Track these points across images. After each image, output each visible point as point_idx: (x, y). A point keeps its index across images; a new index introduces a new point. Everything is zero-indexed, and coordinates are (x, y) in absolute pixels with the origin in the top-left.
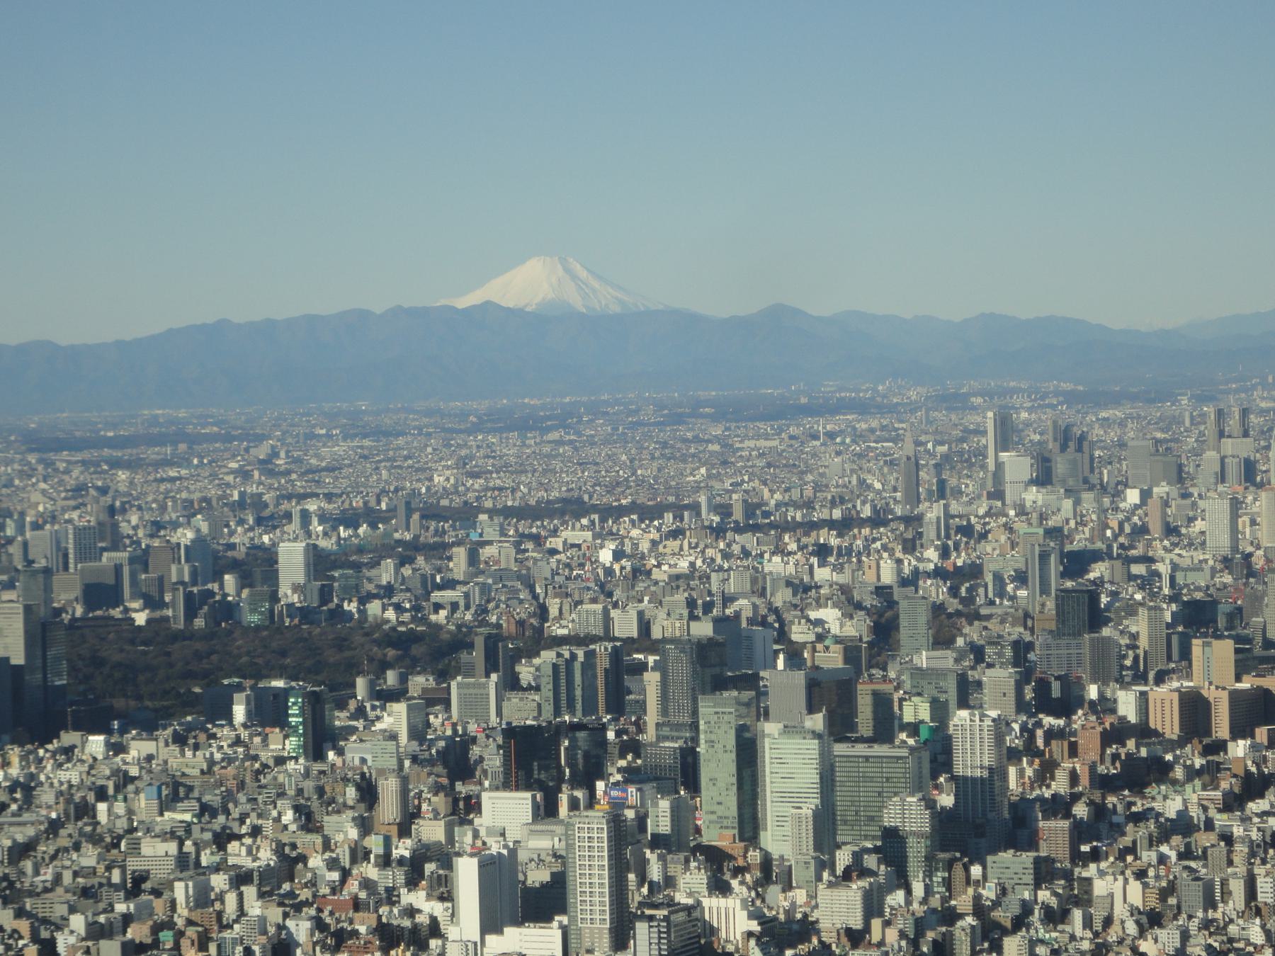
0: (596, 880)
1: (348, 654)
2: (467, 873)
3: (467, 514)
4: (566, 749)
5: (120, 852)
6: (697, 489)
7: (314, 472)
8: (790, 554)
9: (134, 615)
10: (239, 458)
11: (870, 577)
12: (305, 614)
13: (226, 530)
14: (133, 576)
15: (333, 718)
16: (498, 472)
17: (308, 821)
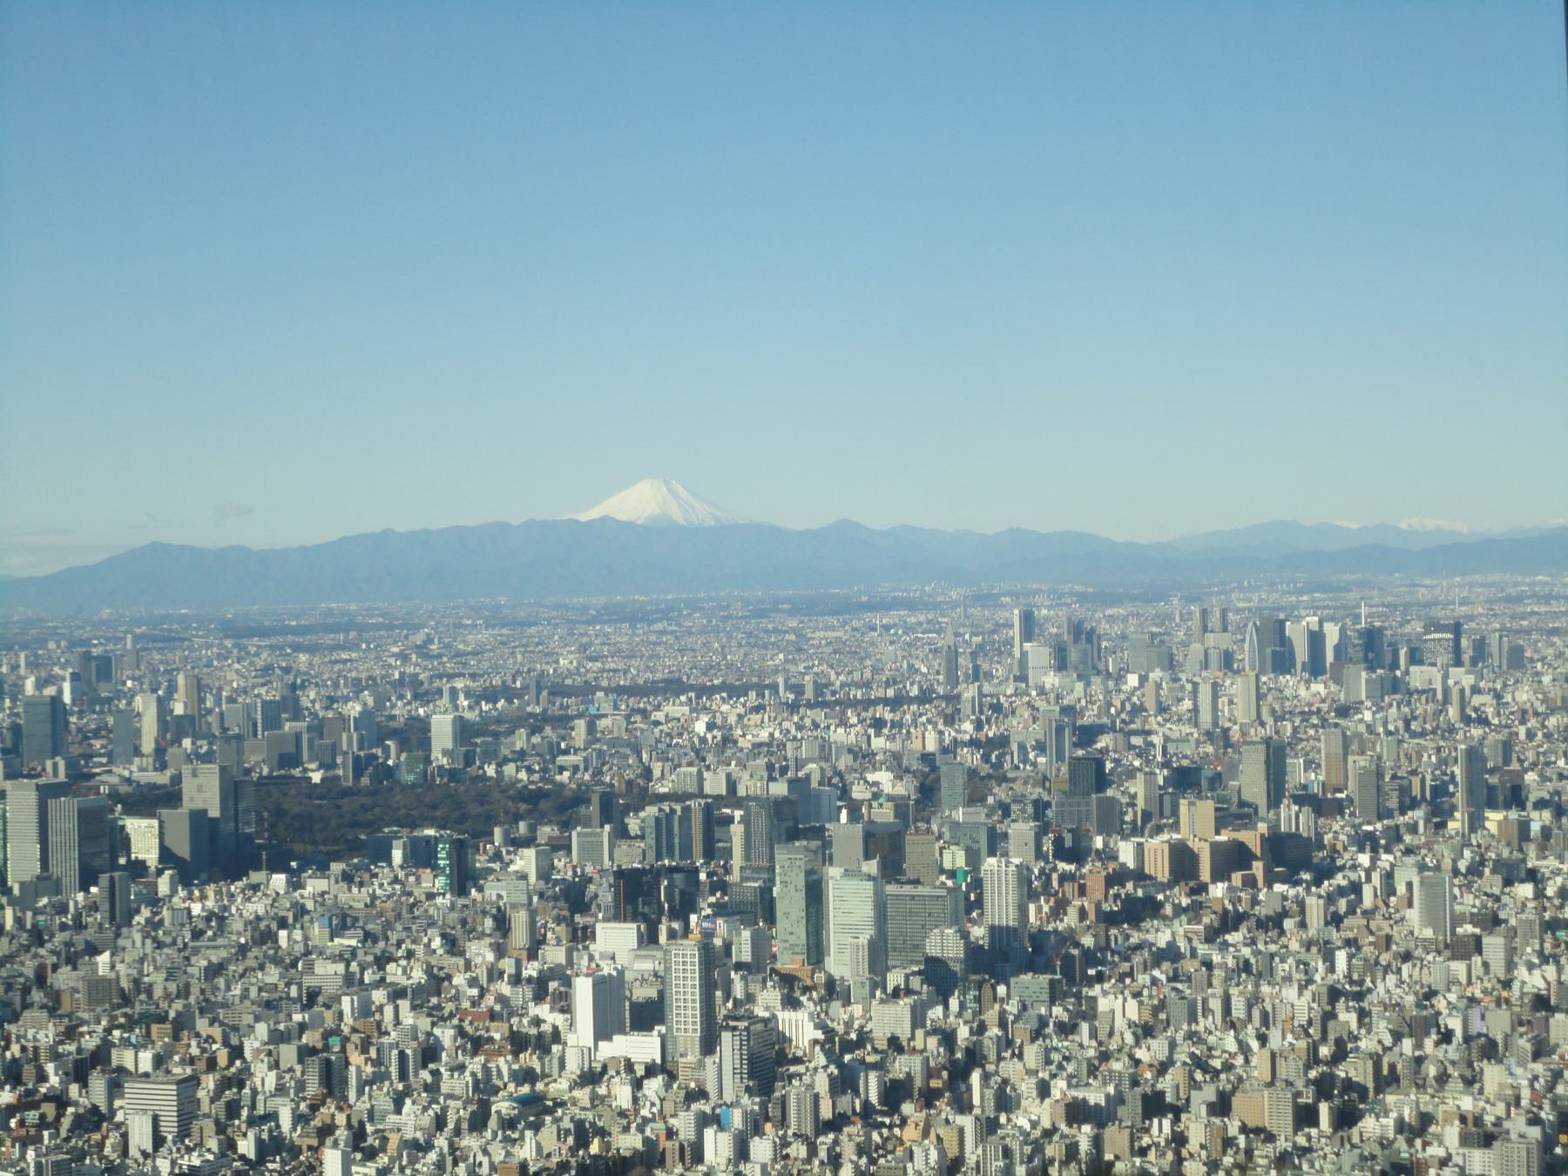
0: (689, 997)
1: (487, 807)
2: (583, 991)
3: (586, 691)
6: (776, 671)
7: (461, 656)
8: (851, 726)
9: (311, 774)
11: (916, 745)
12: (452, 774)
14: (310, 741)
15: (475, 861)
17: (453, 946)
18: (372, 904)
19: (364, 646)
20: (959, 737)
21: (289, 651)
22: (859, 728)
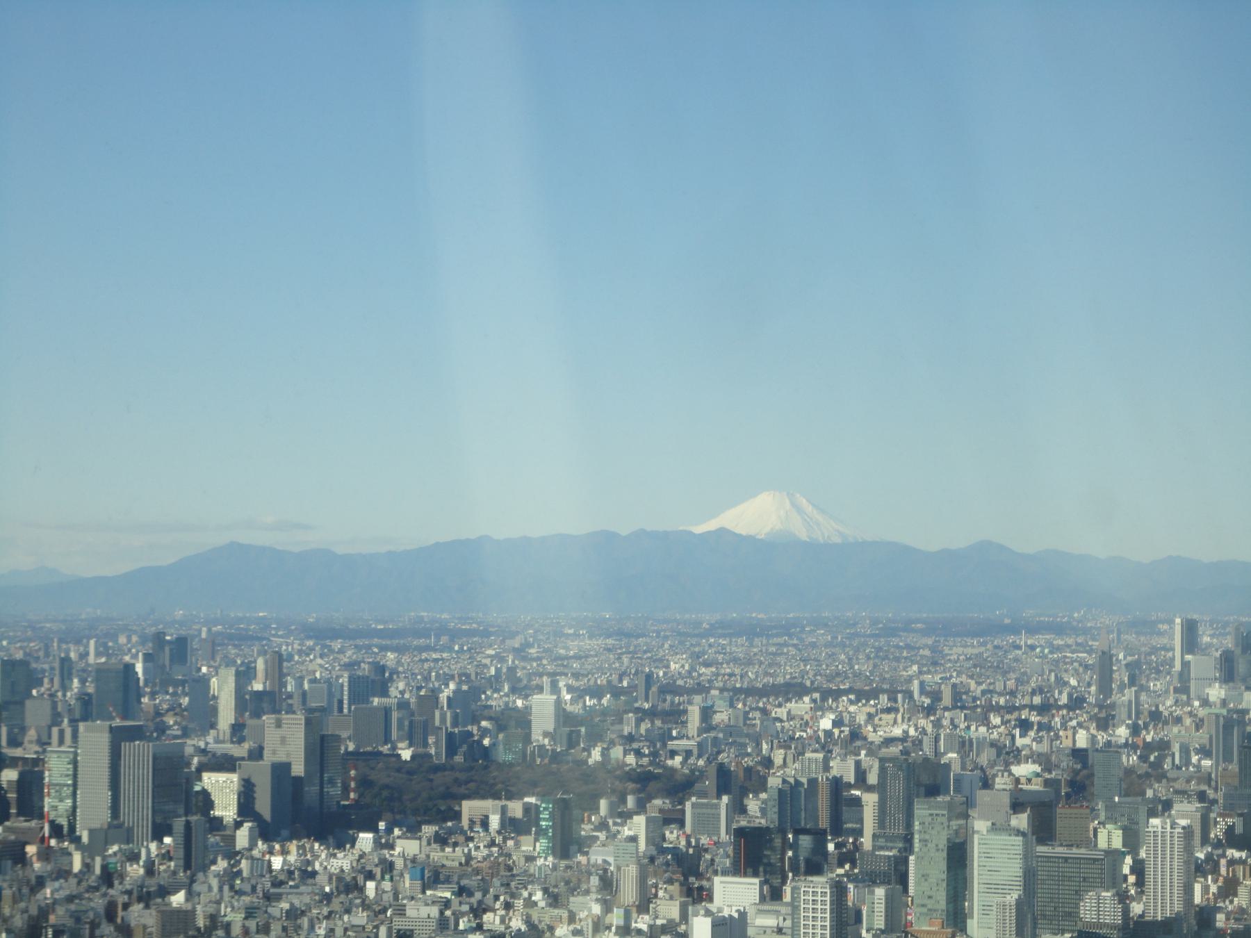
3: (701, 689)
6: (909, 680)
8: (995, 727)
9: (400, 752)
11: (1067, 743)
12: (555, 757)
16: (728, 663)
18: (467, 863)
19: (456, 648)
20: (1114, 739)
21: (376, 650)
22: (1002, 729)
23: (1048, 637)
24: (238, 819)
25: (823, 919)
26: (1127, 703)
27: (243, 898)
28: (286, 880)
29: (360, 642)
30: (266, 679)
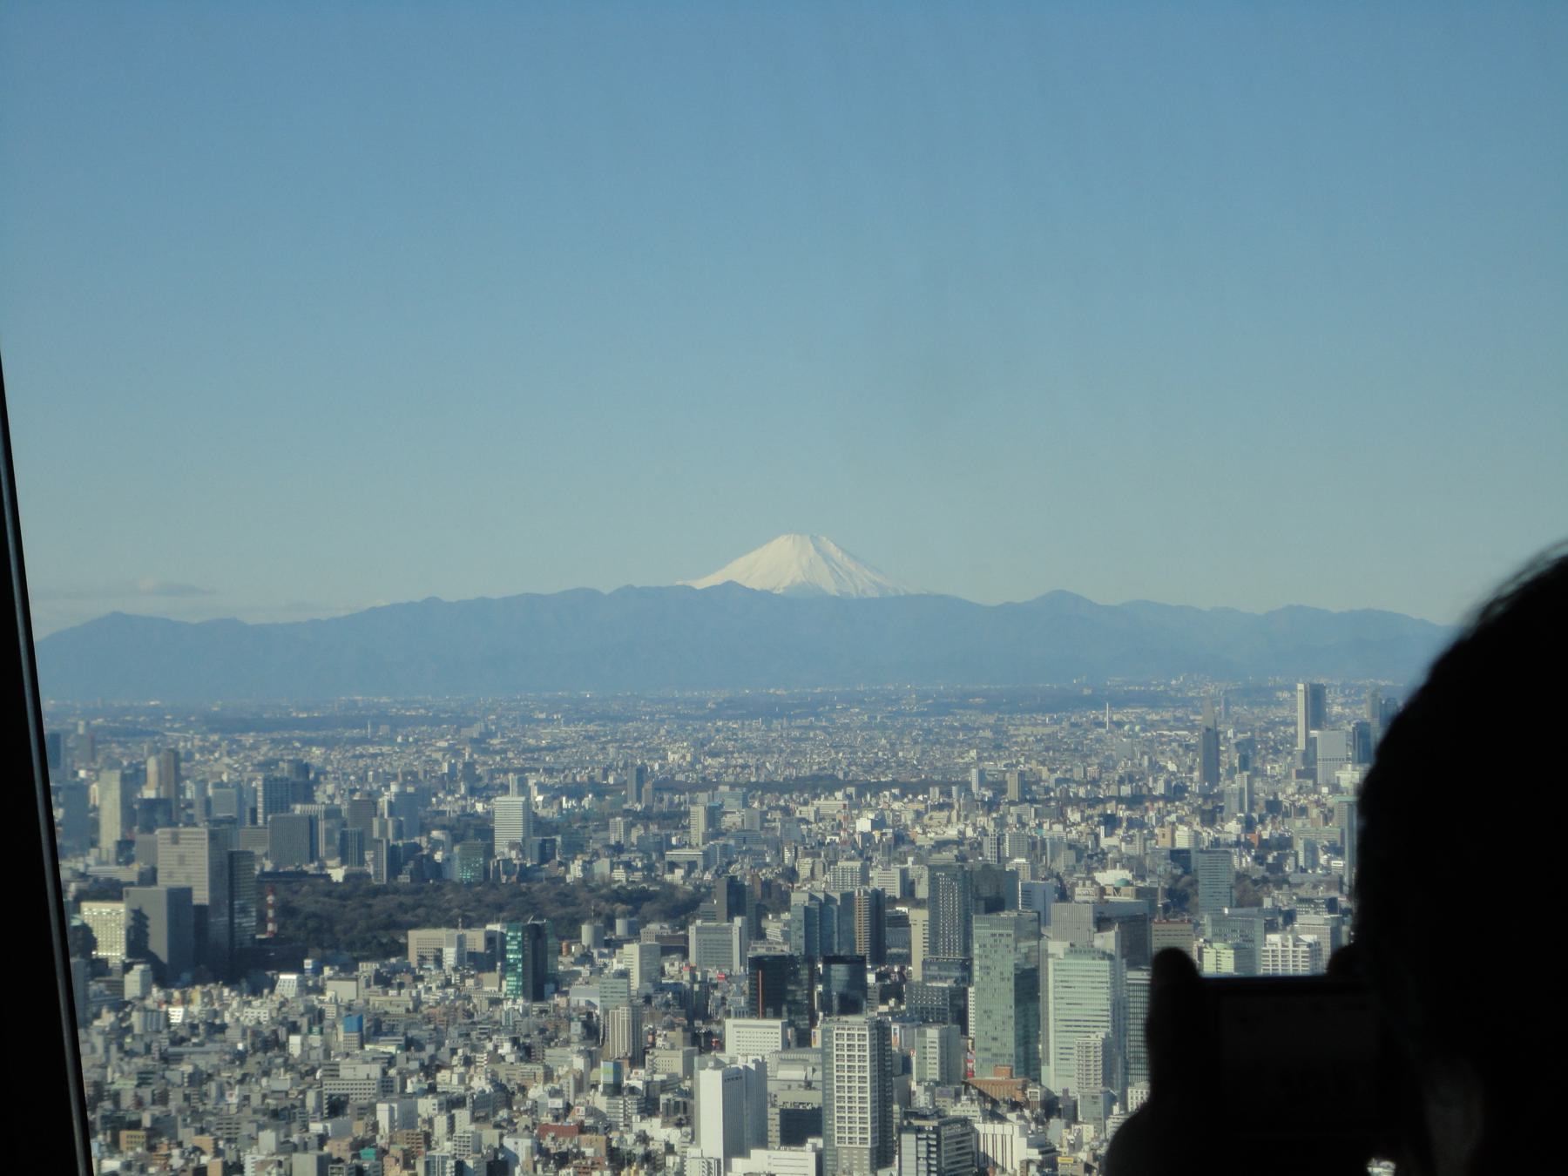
0: (856, 1094)
1: (571, 910)
2: (710, 1088)
3: (707, 785)
4: (820, 994)
5: (315, 1079)
6: (966, 769)
8: (1074, 824)
9: (329, 871)
10: (449, 737)
11: (1165, 843)
12: (525, 874)
13: (434, 800)
16: (740, 753)
18: (416, 1009)
19: (399, 739)
20: (1222, 836)
21: (297, 744)
22: (1082, 827)
23: (1138, 711)
24: (127, 961)
25: (862, 1068)
26: (1237, 792)
27: (135, 1060)
28: (188, 1036)
29: (276, 735)
30: (160, 783)
